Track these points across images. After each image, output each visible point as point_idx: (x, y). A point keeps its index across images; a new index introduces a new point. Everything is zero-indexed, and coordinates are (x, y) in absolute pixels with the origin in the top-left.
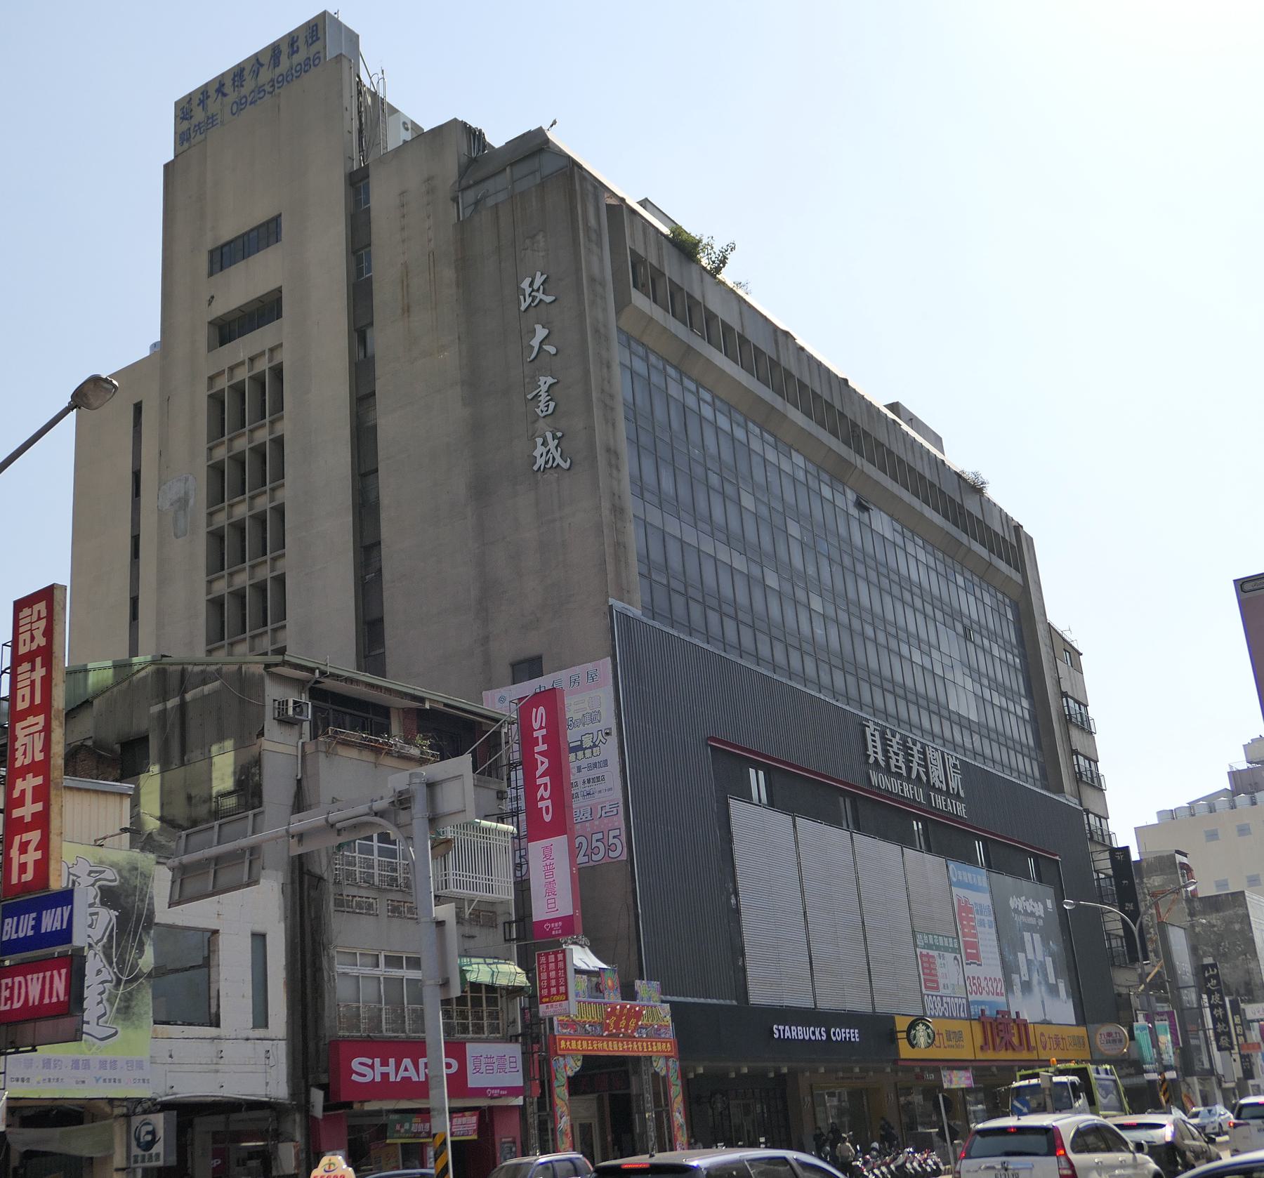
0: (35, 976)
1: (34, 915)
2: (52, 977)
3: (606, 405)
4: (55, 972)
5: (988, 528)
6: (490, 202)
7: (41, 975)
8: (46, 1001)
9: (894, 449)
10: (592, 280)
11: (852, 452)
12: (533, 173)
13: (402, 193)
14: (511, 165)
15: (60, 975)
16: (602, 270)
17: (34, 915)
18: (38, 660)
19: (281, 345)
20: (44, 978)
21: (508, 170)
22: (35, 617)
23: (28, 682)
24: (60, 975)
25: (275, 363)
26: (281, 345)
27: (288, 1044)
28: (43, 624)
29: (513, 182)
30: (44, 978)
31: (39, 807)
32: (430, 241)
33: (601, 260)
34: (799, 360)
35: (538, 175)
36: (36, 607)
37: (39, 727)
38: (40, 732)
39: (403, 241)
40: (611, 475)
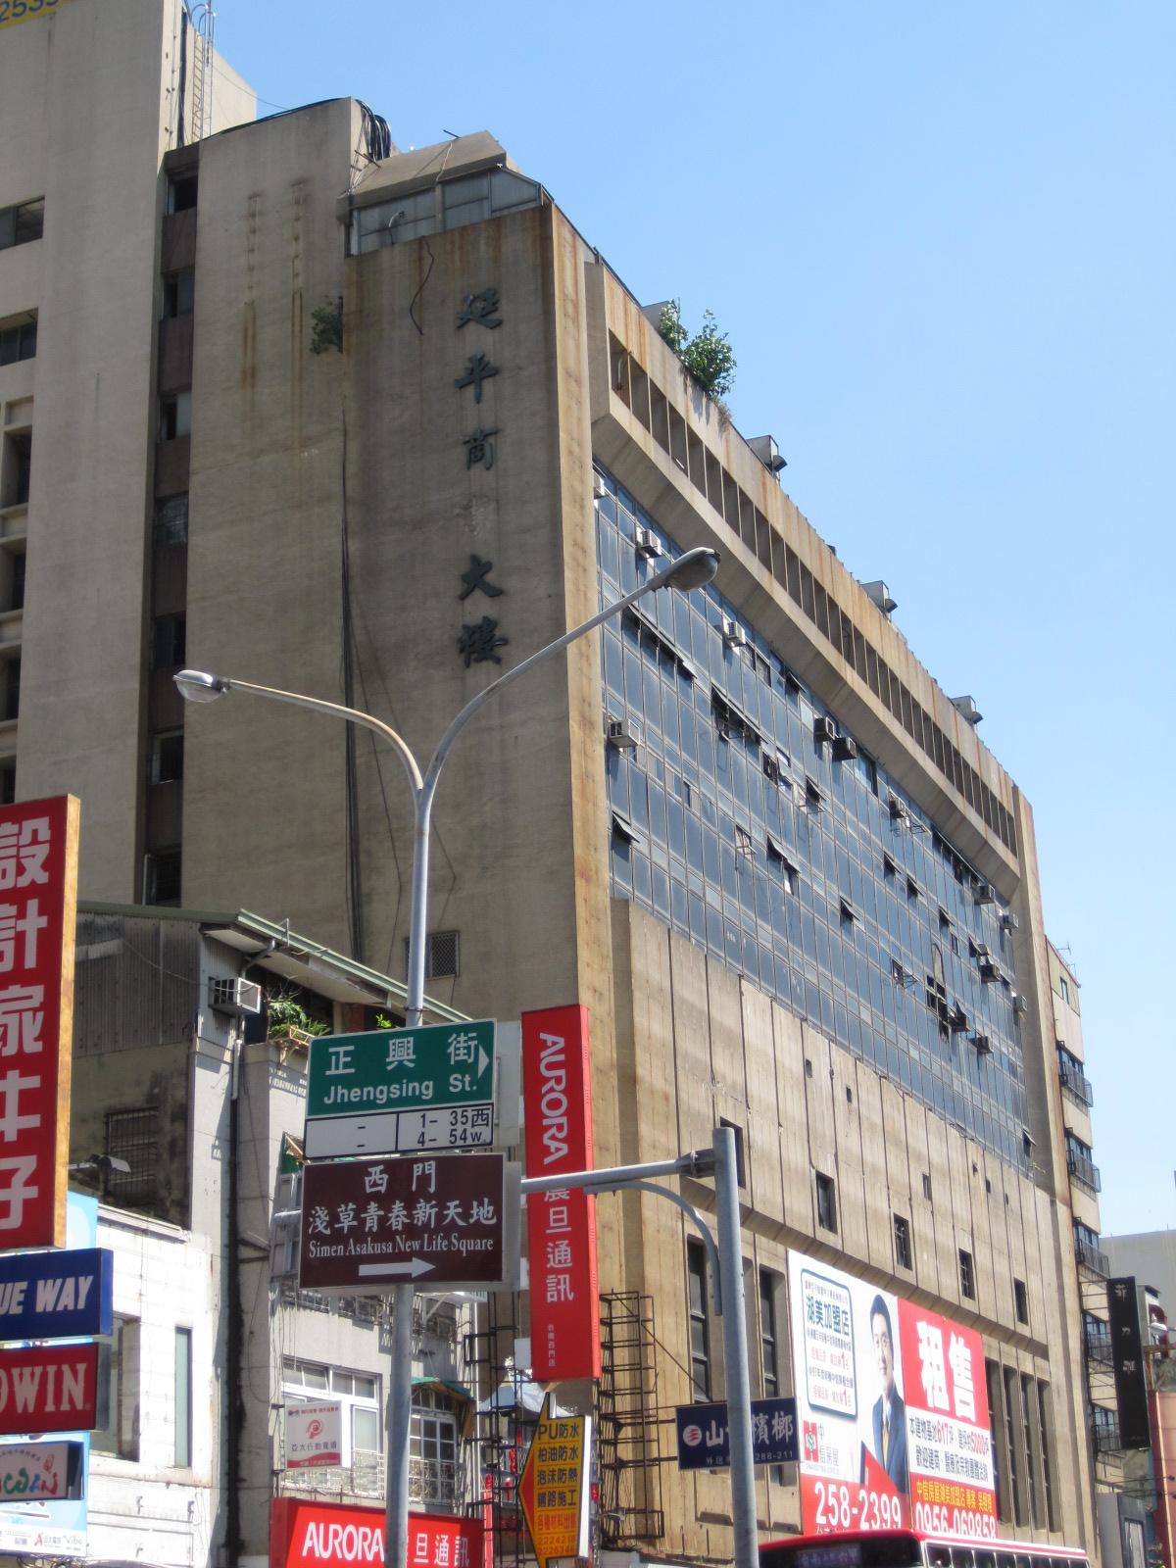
0: (27, 1371)
1: (24, 1285)
2: (59, 1376)
3: (578, 565)
4: (66, 1368)
5: (985, 787)
6: (408, 234)
7: (38, 1370)
8: (50, 1407)
9: (887, 660)
10: (568, 374)
11: (842, 659)
12: (481, 200)
13: (253, 197)
14: (444, 183)
15: (75, 1373)
16: (579, 362)
17: (24, 1285)
18: (33, 905)
19: (30, 400)
20: (44, 1375)
21: (438, 190)
22: (26, 838)
23: (11, 933)
24: (75, 1373)
25: (18, 424)
26: (30, 400)
27: (1118, 1401)
28: (42, 852)
29: (445, 209)
30: (44, 1375)
31: (33, 1121)
32: (296, 276)
33: (578, 346)
34: (787, 516)
35: (486, 204)
36: (29, 826)
37: (36, 1002)
38: (35, 1010)
39: (251, 269)
40: (581, 669)
